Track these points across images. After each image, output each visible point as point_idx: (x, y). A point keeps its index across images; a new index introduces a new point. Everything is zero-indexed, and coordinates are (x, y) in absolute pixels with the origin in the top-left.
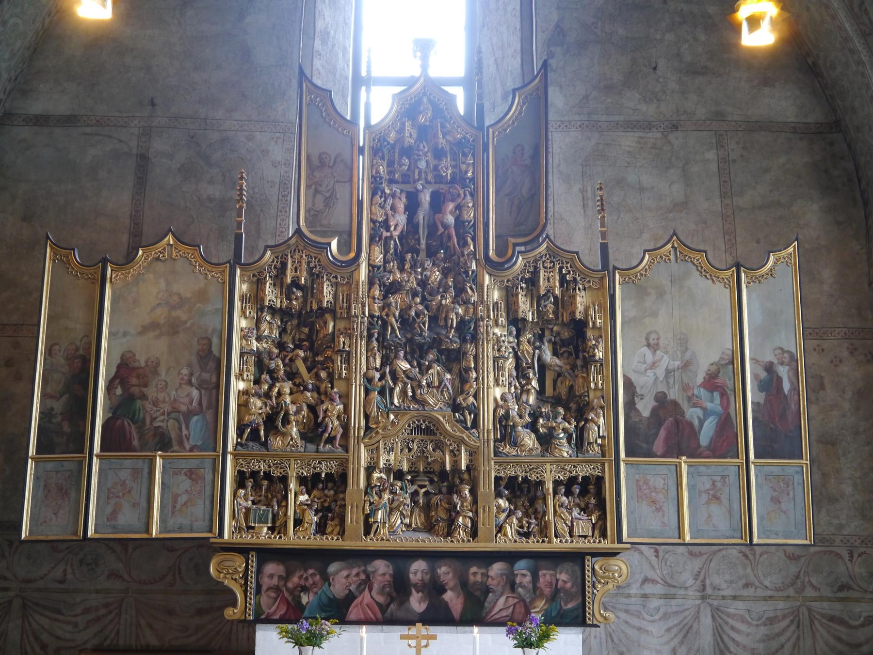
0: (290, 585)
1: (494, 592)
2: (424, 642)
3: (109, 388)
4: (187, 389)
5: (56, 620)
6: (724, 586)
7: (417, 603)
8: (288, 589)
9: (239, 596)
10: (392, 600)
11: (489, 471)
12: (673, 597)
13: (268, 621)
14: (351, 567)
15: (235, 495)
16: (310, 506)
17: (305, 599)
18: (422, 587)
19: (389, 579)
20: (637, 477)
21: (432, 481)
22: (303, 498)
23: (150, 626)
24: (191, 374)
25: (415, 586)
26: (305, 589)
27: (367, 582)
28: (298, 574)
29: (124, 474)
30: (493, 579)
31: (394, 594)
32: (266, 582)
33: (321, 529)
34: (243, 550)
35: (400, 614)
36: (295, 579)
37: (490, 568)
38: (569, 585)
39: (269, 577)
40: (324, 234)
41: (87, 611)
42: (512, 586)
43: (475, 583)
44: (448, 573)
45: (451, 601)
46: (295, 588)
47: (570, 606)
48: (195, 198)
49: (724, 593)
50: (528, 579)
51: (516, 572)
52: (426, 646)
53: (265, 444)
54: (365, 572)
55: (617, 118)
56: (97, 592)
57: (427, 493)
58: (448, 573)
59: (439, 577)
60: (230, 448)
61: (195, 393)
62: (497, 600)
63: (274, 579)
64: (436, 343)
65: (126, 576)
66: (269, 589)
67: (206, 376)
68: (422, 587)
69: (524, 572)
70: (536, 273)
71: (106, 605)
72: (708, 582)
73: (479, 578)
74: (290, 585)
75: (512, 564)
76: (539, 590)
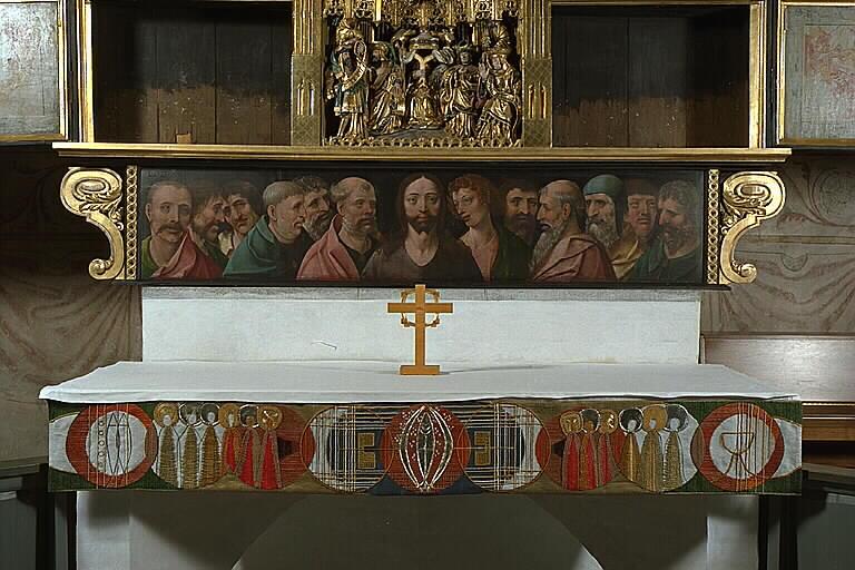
0: (199, 221)
1: (549, 230)
2: (429, 318)
7: (417, 250)
10: (375, 245)
12: (831, 240)
13: (166, 281)
14: (303, 191)
17: (226, 245)
18: (427, 224)
19: (370, 211)
20: (807, 30)
21: (442, 43)
25: (414, 221)
26: (227, 228)
27: (332, 214)
28: (212, 203)
30: (547, 209)
32: (157, 215)
35: (391, 268)
36: (208, 212)
37: (543, 190)
38: (678, 219)
39: (162, 207)
42: (581, 221)
43: (518, 216)
44: (471, 199)
45: (476, 247)
46: (212, 224)
47: (679, 254)
50: (609, 208)
51: (587, 198)
52: (436, 323)
54: (327, 197)
57: (433, 64)
58: (471, 199)
59: (455, 206)
62: (555, 244)
63: (171, 212)
66: (160, 230)
68: (427, 224)
69: (601, 196)
73: (523, 208)
74: (199, 221)
75: (582, 184)
76: (627, 228)
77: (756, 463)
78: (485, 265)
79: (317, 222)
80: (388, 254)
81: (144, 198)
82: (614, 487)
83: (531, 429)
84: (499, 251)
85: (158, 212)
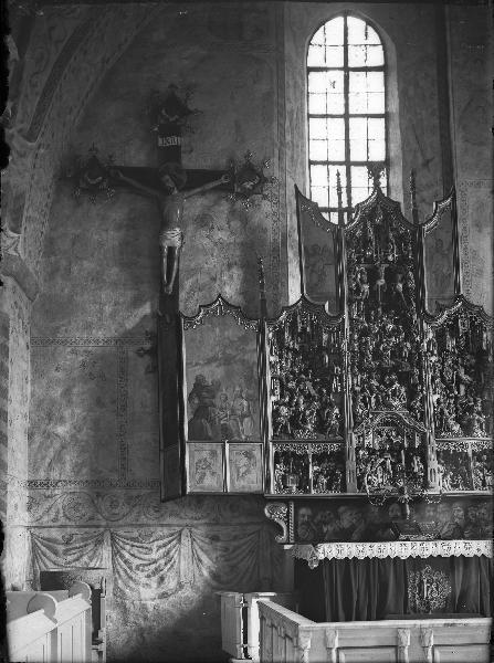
3: (190, 399)
4: (240, 401)
9: (284, 526)
11: (433, 445)
15: (275, 468)
16: (321, 473)
22: (316, 468)
24: (242, 391)
26: (325, 524)
29: (205, 454)
33: (329, 487)
34: (286, 501)
36: (319, 517)
38: (486, 516)
40: (318, 299)
53: (292, 435)
60: (270, 438)
61: (245, 403)
64: (395, 369)
66: (303, 524)
67: (251, 392)
70: (456, 320)
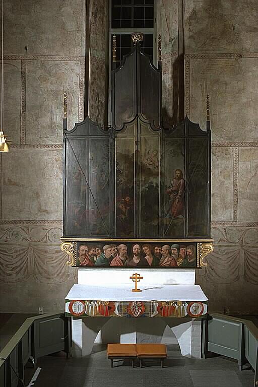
1: (164, 256)
2: (138, 280)
5: (5, 255)
6: (250, 242)
7: (136, 260)
8: (89, 255)
12: (231, 246)
14: (112, 247)
23: (39, 257)
26: (95, 255)
31: (127, 257)
35: (130, 264)
36: (92, 252)
41: (16, 251)
48: (46, 90)
49: (250, 245)
50: (176, 251)
54: (117, 249)
55: (217, 52)
56: (19, 245)
59: (144, 251)
65: (29, 239)
69: (175, 249)
71: (22, 250)
72: (244, 241)
73: (158, 251)
77: (199, 312)
78: (150, 264)
79: (114, 254)
80: (130, 261)
81: (78, 249)
82: (171, 316)
83: (156, 305)
84: (153, 261)
85: (81, 252)
